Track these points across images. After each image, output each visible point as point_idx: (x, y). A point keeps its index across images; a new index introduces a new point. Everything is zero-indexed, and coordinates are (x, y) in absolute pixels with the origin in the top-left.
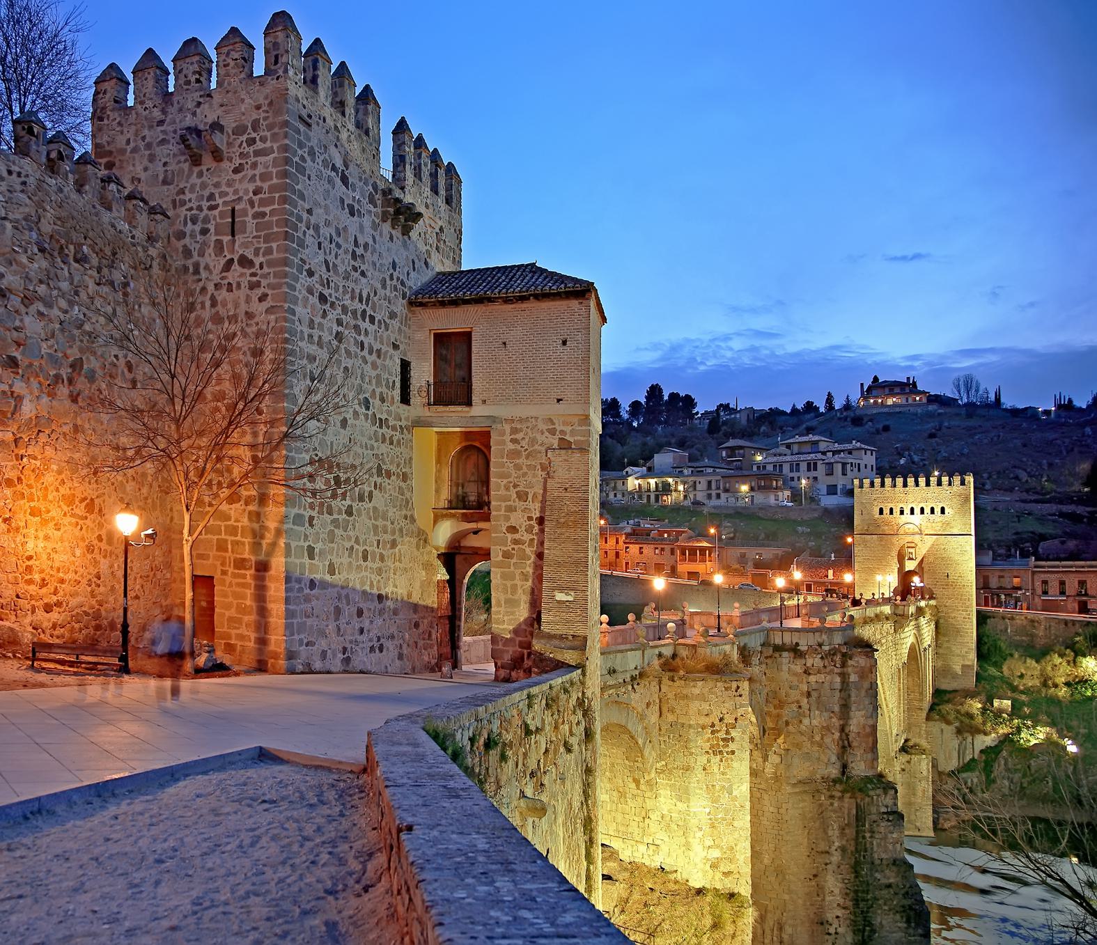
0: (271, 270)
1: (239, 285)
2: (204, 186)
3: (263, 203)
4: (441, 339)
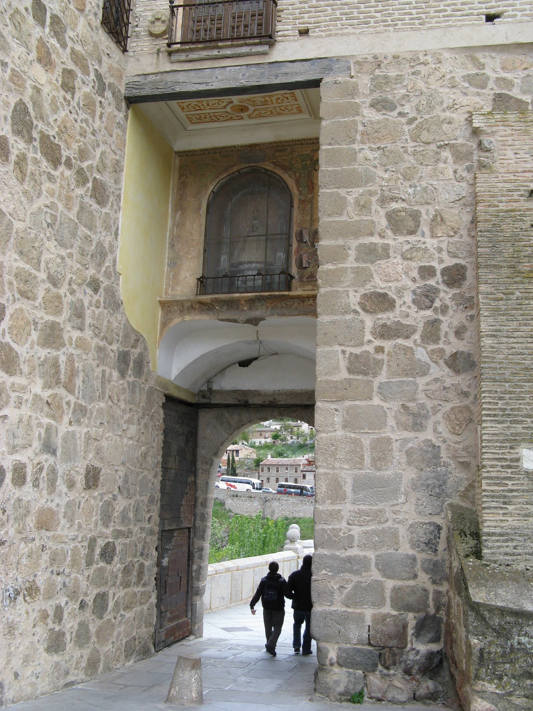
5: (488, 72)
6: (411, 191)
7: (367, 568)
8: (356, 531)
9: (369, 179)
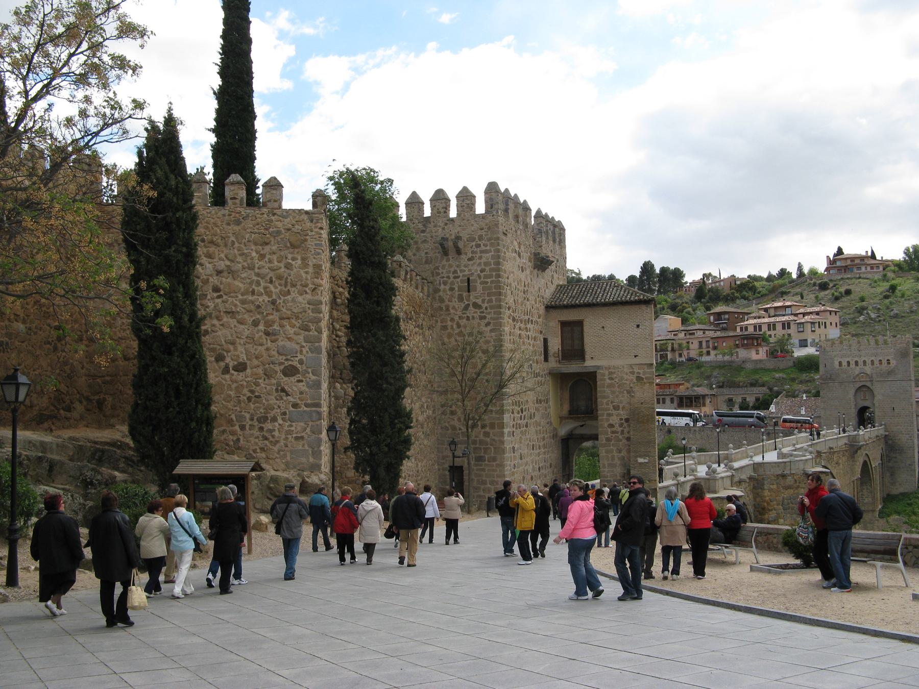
0: (492, 311)
2: (450, 266)
3: (486, 277)
4: (564, 324)
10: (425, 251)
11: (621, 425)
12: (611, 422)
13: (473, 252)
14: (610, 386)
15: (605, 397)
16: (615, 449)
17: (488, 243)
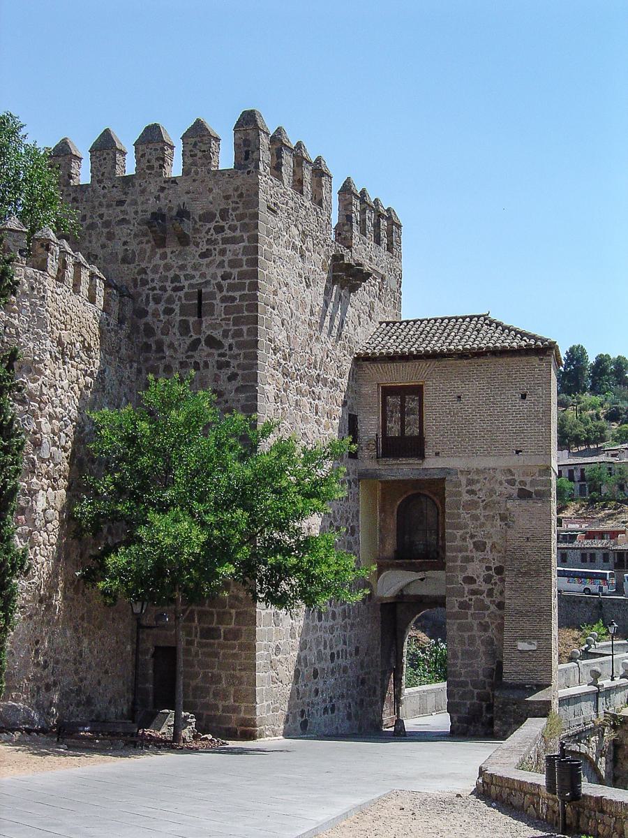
0: (242, 352)
1: (206, 365)
3: (232, 287)
4: (387, 391)
5: (516, 477)
6: (482, 533)
7: (467, 685)
8: (463, 671)
9: (466, 526)
10: (124, 239)
11: (488, 579)
12: (469, 573)
13: (209, 242)
14: (474, 504)
15: (458, 527)
16: (475, 622)
17: (238, 224)
